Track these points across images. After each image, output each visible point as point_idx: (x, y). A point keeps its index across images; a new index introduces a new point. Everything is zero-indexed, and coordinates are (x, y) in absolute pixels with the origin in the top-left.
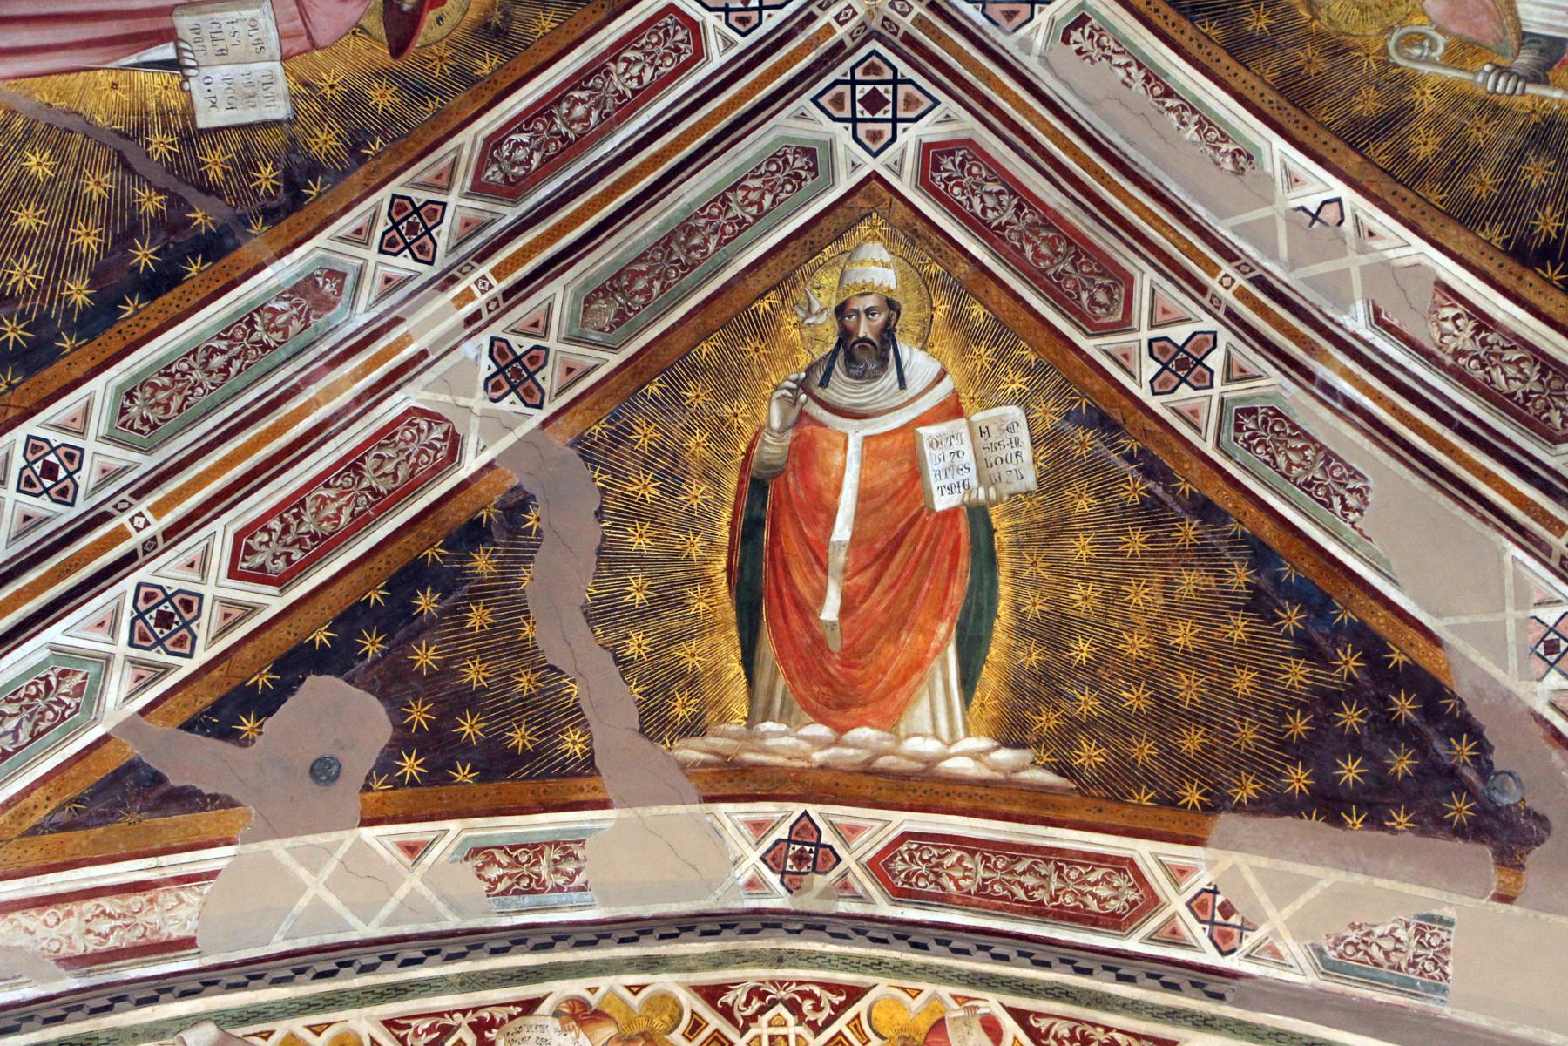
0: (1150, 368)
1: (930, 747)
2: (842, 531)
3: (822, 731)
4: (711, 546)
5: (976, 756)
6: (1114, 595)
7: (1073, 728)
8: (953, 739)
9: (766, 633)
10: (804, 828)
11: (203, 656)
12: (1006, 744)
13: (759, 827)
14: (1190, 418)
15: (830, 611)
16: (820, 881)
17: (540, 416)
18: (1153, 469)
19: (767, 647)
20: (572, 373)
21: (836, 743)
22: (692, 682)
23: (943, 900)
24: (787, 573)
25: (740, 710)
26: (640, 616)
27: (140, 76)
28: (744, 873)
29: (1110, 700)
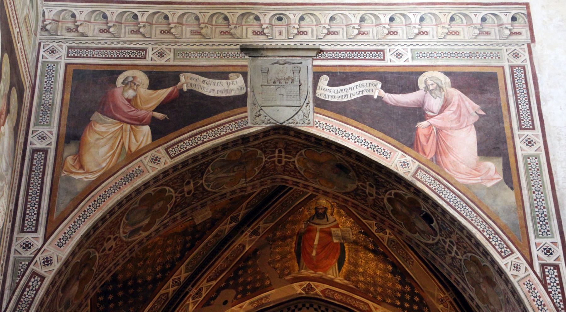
0: (375, 228)
1: (333, 277)
2: (316, 242)
3: (312, 272)
4: (291, 248)
5: (341, 280)
6: (367, 263)
7: (358, 281)
8: (336, 277)
9: (302, 258)
10: (309, 285)
11: (203, 296)
12: (346, 279)
13: (301, 286)
14: (383, 239)
15: (314, 254)
16: (312, 293)
17: (259, 237)
18: (374, 245)
19: (302, 260)
20: (265, 228)
21: (315, 273)
22: (288, 268)
23: (334, 300)
24: (306, 249)
25: (297, 268)
26: (278, 261)
27: (187, 223)
28: (298, 292)
29: (366, 279)
